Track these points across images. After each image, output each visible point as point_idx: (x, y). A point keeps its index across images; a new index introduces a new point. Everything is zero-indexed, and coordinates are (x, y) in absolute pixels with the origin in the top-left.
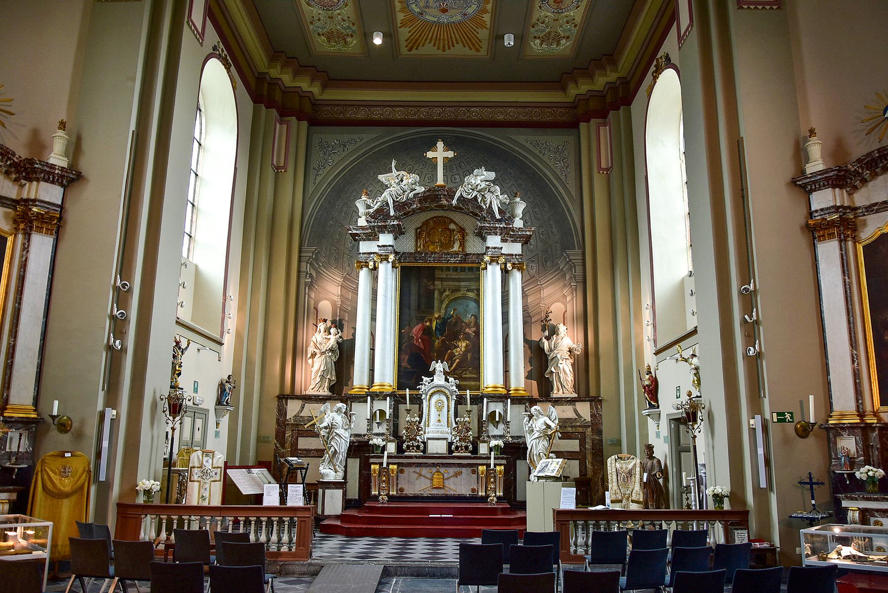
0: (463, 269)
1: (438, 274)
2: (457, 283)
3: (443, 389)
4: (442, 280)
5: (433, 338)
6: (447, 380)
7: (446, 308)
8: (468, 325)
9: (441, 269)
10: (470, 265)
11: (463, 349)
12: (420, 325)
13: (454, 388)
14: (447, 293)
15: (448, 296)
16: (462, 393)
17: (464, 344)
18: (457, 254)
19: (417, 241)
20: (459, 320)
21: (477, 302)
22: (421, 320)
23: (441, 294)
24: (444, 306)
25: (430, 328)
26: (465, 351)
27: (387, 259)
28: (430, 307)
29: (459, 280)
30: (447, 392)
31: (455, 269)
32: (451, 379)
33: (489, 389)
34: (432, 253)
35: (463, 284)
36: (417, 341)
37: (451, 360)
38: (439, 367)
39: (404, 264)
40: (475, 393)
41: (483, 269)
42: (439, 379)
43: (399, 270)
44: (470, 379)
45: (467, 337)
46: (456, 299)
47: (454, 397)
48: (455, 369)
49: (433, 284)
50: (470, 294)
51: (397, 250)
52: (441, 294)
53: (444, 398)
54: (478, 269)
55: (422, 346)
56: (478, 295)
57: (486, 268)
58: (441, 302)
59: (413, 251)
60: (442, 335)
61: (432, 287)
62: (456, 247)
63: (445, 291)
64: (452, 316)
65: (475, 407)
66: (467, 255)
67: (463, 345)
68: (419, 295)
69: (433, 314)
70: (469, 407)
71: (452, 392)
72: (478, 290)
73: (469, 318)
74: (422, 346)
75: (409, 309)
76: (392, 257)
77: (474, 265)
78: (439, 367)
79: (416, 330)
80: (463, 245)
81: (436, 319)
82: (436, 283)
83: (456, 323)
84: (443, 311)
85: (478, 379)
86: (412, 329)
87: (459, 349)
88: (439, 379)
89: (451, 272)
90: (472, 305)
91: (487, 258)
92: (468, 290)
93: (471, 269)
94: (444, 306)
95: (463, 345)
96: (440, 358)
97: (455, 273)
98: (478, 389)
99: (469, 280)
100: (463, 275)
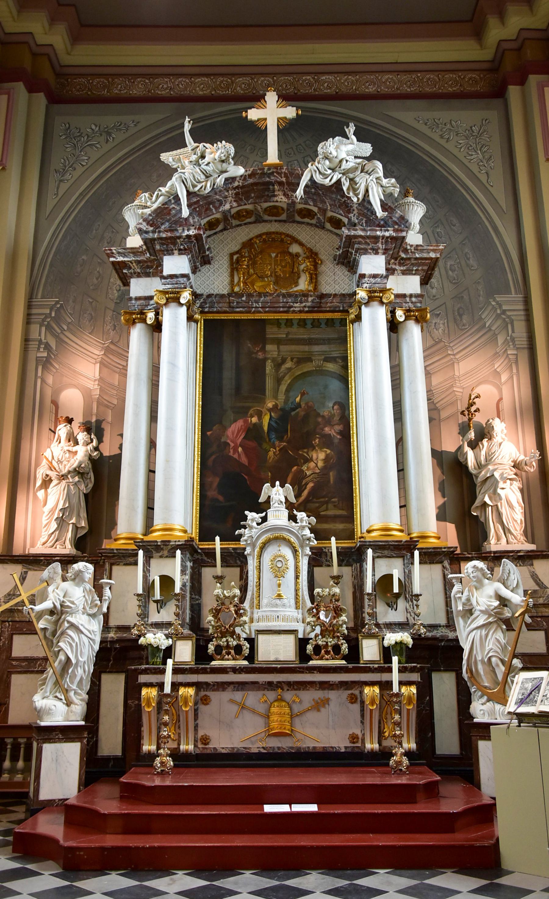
0: (316, 323)
1: (271, 332)
2: (306, 348)
3: (286, 535)
4: (279, 342)
5: (265, 446)
6: (292, 518)
7: (288, 391)
8: (328, 422)
9: (277, 323)
10: (329, 316)
11: (320, 464)
12: (240, 423)
13: (307, 532)
14: (289, 364)
15: (290, 369)
16: (323, 544)
17: (322, 456)
18: (305, 295)
19: (232, 276)
20: (311, 413)
21: (344, 379)
22: (242, 412)
23: (278, 366)
24: (283, 387)
25: (258, 427)
26: (325, 468)
27: (177, 300)
28: (259, 391)
29: (310, 342)
30: (293, 539)
31: (302, 323)
32: (301, 515)
33: (374, 534)
34: (260, 295)
35: (316, 348)
36: (235, 450)
37: (298, 485)
38: (277, 494)
39: (210, 317)
40: (346, 544)
41: (353, 322)
42: (278, 516)
43: (201, 325)
44: (335, 518)
45: (327, 442)
46: (304, 375)
47: (308, 551)
48: (307, 501)
49: (263, 349)
50: (331, 367)
51: (198, 292)
52: (278, 366)
53: (287, 552)
54: (343, 323)
55: (244, 460)
56: (345, 367)
57: (358, 318)
58: (279, 381)
59: (225, 292)
60: (281, 439)
61: (260, 356)
62: (303, 284)
63: (284, 361)
64: (299, 405)
65: (347, 571)
66: (322, 296)
67: (319, 456)
68: (238, 370)
69: (262, 401)
70: (335, 569)
71: (303, 541)
72: (345, 359)
73: (329, 408)
74: (244, 460)
75: (221, 394)
76: (185, 297)
77: (337, 316)
78: (277, 494)
79: (234, 431)
80: (314, 278)
81: (270, 410)
82: (269, 347)
83: (306, 417)
84: (282, 397)
85: (350, 518)
86: (225, 428)
87: (312, 465)
88: (278, 516)
89: (295, 329)
90: (335, 385)
91: (362, 294)
92: (327, 360)
93: (330, 323)
94: (283, 387)
95: (319, 456)
96: (279, 476)
97: (302, 330)
98: (351, 535)
99: (328, 341)
100: (316, 334)
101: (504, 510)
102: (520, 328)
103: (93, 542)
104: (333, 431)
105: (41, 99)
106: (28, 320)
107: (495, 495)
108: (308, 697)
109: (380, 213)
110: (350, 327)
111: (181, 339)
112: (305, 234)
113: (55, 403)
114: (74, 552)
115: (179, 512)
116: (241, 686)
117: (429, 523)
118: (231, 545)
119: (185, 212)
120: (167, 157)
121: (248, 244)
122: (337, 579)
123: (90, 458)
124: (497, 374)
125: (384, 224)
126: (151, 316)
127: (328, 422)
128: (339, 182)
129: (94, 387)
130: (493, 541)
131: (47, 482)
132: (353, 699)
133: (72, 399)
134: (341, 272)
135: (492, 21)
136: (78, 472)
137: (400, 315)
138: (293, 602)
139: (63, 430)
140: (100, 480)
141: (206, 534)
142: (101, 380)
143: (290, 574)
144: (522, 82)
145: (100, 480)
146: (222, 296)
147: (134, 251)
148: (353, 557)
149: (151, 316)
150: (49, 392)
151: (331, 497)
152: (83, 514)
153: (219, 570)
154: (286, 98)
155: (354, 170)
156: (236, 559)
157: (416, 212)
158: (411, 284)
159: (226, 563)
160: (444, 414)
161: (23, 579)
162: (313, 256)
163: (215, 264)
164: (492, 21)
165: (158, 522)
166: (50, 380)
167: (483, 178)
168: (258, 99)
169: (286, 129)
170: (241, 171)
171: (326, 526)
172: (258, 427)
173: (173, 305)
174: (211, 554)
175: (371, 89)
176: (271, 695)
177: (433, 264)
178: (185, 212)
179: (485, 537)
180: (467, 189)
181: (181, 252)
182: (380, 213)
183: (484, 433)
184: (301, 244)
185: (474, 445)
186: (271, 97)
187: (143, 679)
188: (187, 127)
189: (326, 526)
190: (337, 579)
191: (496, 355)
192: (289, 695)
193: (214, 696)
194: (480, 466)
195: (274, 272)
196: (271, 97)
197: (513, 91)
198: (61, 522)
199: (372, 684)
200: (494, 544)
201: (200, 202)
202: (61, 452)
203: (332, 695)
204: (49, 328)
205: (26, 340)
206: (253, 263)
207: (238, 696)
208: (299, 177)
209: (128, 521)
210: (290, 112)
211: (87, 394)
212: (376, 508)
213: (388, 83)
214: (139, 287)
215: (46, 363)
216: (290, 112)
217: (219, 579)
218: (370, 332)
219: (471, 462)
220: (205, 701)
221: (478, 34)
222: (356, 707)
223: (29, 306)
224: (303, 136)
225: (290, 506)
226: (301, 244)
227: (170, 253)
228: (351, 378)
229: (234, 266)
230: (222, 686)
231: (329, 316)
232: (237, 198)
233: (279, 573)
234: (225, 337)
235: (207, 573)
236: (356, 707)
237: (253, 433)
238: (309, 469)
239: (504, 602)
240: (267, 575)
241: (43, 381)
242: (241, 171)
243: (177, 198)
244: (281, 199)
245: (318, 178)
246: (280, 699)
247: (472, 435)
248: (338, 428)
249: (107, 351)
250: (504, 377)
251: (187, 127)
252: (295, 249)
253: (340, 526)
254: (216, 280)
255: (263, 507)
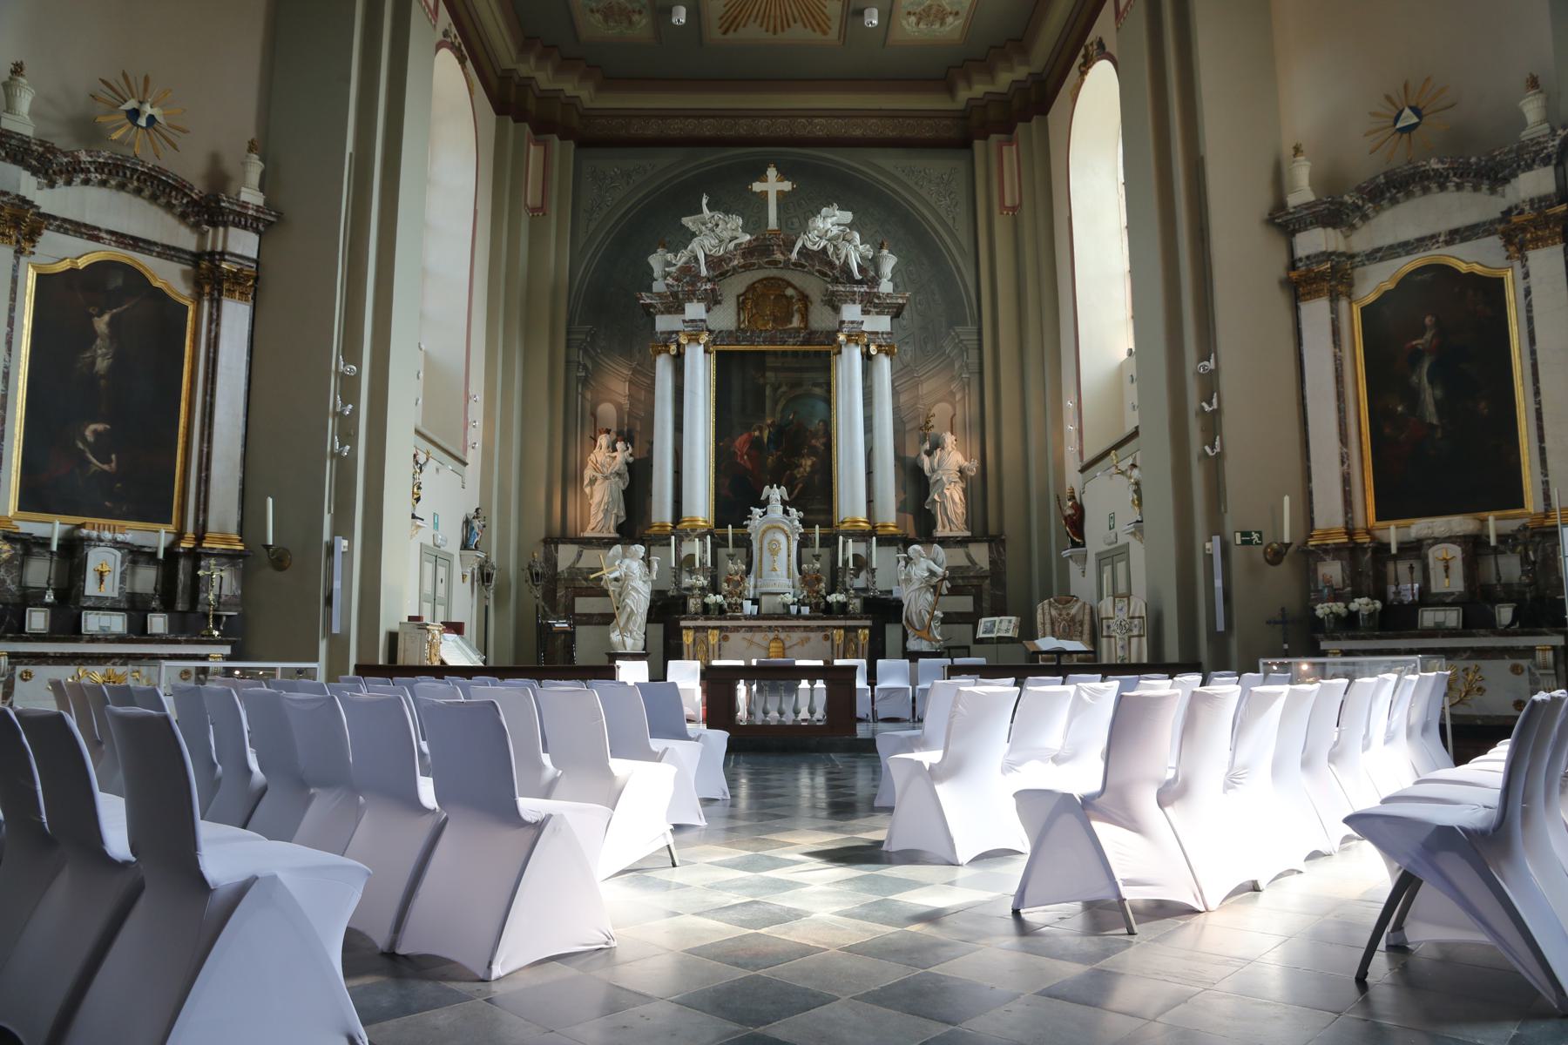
1: (770, 362)
4: (775, 369)
6: (786, 512)
8: (815, 435)
10: (817, 348)
12: (745, 436)
14: (784, 389)
17: (809, 463)
18: (798, 330)
21: (828, 400)
22: (747, 428)
24: (780, 407)
25: (760, 439)
28: (760, 411)
32: (793, 511)
35: (806, 375)
39: (721, 348)
42: (776, 510)
45: (813, 451)
49: (763, 376)
50: (818, 391)
52: (775, 389)
53: (782, 538)
54: (828, 354)
55: (749, 465)
56: (829, 391)
58: (776, 402)
61: (761, 381)
62: (796, 322)
63: (780, 386)
66: (812, 333)
67: (808, 463)
70: (817, 550)
72: (829, 385)
73: (816, 424)
74: (749, 465)
78: (776, 494)
79: (740, 442)
80: (805, 317)
82: (769, 374)
84: (778, 416)
88: (776, 510)
90: (821, 406)
94: (780, 407)
95: (808, 463)
101: (949, 506)
102: (974, 354)
103: (634, 526)
104: (818, 443)
105: (571, 145)
106: (568, 346)
107: (942, 494)
108: (796, 636)
109: (858, 276)
110: (833, 358)
111: (700, 368)
112: (796, 278)
113: (594, 415)
114: (614, 535)
115: (700, 505)
116: (750, 629)
117: (888, 514)
118: (740, 531)
119: (704, 272)
120: (687, 221)
121: (751, 288)
122: (817, 557)
123: (627, 464)
124: (952, 394)
125: (859, 282)
126: (673, 348)
127: (815, 435)
128: (825, 247)
129: (625, 402)
130: (939, 528)
131: (593, 481)
132: (826, 638)
133: (607, 411)
134: (828, 310)
135: (961, 85)
136: (618, 474)
137: (873, 350)
138: (785, 573)
139: (603, 440)
140: (638, 479)
141: (720, 521)
142: (630, 396)
143: (784, 553)
144: (986, 138)
145: (638, 479)
146: (731, 332)
147: (659, 295)
148: (829, 541)
149: (673, 348)
150: (588, 406)
151: (814, 498)
152: (622, 505)
153: (731, 550)
154: (784, 175)
155: (836, 237)
156: (744, 542)
157: (889, 263)
158: (883, 323)
159: (736, 545)
160: (908, 427)
161: (580, 555)
162: (805, 298)
163: (725, 305)
164: (961, 85)
165: (686, 513)
166: (589, 396)
167: (950, 222)
168: (761, 176)
169: (781, 195)
170: (748, 237)
171: (811, 517)
172: (760, 439)
173: (693, 344)
174: (725, 538)
175: (858, 133)
176: (771, 635)
177: (902, 307)
178: (704, 272)
179: (934, 526)
180: (936, 232)
181: (699, 300)
182: (858, 276)
183: (937, 445)
184: (795, 288)
185: (929, 453)
186: (772, 173)
187: (683, 623)
188: (704, 201)
189: (811, 517)
190: (817, 557)
191: (953, 378)
192: (782, 635)
193: (732, 635)
194: (933, 471)
195: (772, 313)
196: (772, 173)
197: (978, 145)
198: (606, 511)
199: (839, 627)
200: (940, 532)
201: (712, 262)
202: (605, 460)
203: (812, 635)
204: (586, 351)
205: (568, 362)
206: (756, 305)
207: (749, 635)
208: (794, 244)
209: (662, 511)
210: (787, 186)
211: (619, 407)
212: (851, 504)
213: (873, 128)
214: (663, 323)
215: (585, 382)
216: (787, 186)
217: (731, 557)
218: (850, 364)
219: (927, 467)
220: (726, 638)
221: (951, 90)
222: (828, 643)
223: (569, 332)
224: (799, 208)
225: (784, 503)
226: (795, 288)
227: (690, 300)
228: (833, 401)
229: (741, 307)
230: (737, 629)
231: (817, 348)
232: (744, 255)
233: (774, 552)
234: (732, 369)
235: (722, 552)
236: (828, 643)
237: (756, 444)
238: (799, 473)
239: (932, 573)
240: (766, 554)
241: (583, 397)
242: (748, 237)
243: (696, 259)
244: (779, 256)
245: (809, 245)
246: (776, 639)
247: (927, 446)
248: (823, 440)
249: (635, 371)
250: (958, 397)
251: (704, 201)
252: (790, 292)
253: (822, 517)
254: (725, 318)
255: (763, 504)
